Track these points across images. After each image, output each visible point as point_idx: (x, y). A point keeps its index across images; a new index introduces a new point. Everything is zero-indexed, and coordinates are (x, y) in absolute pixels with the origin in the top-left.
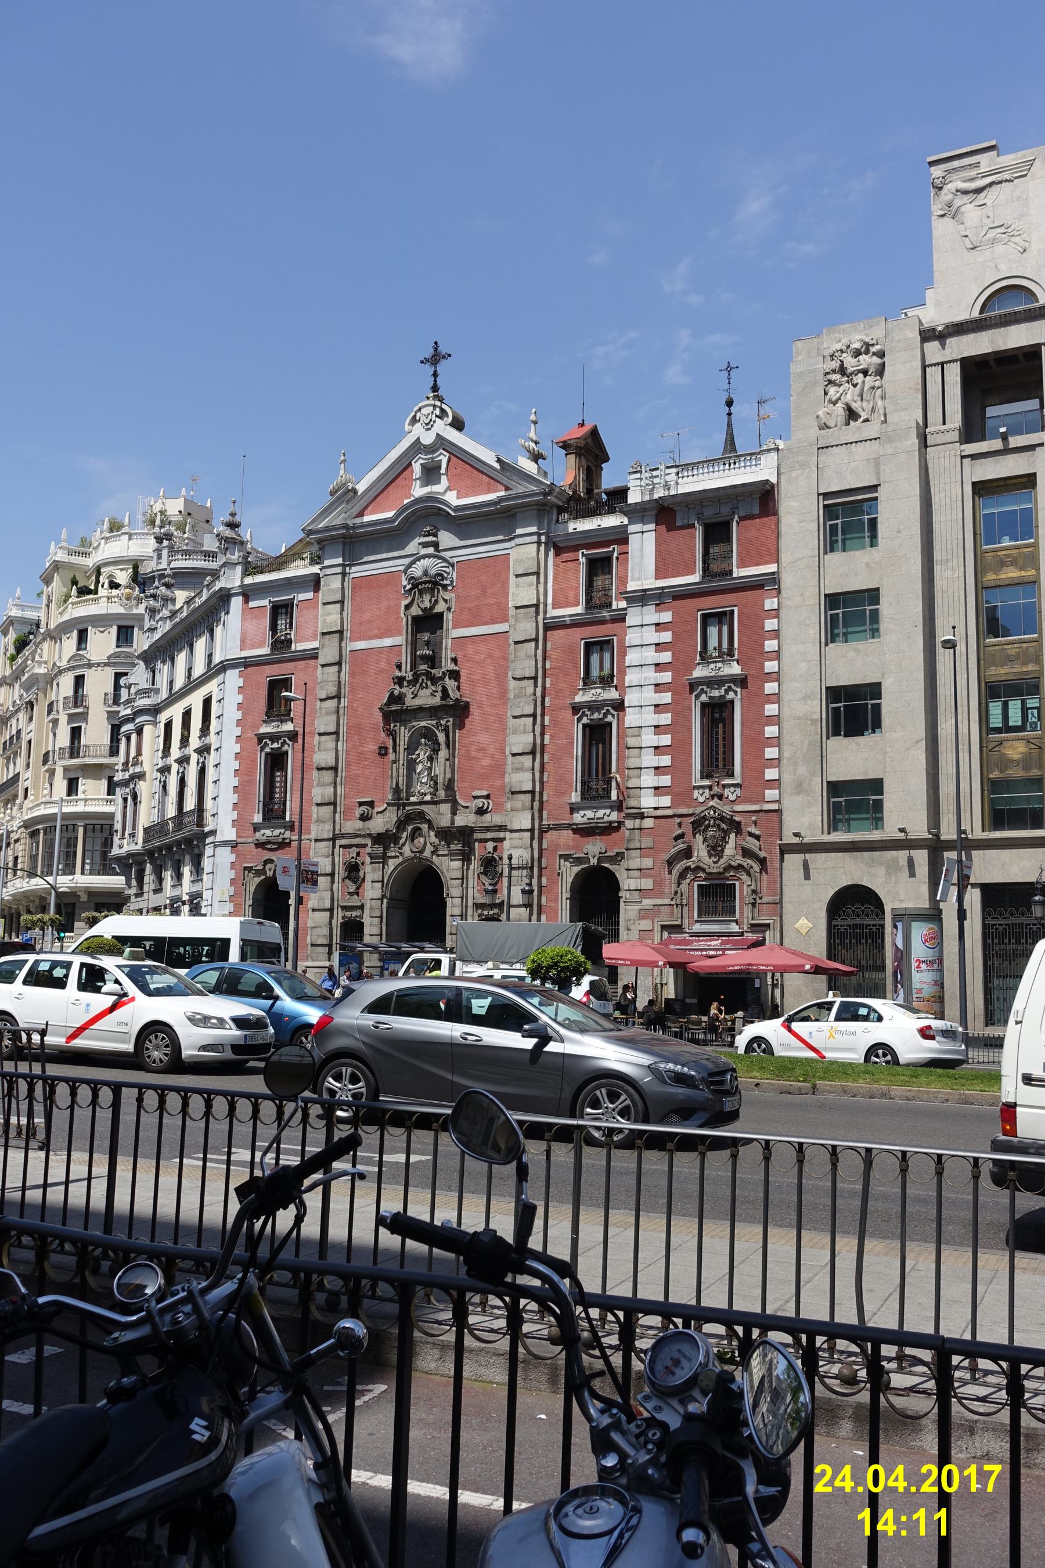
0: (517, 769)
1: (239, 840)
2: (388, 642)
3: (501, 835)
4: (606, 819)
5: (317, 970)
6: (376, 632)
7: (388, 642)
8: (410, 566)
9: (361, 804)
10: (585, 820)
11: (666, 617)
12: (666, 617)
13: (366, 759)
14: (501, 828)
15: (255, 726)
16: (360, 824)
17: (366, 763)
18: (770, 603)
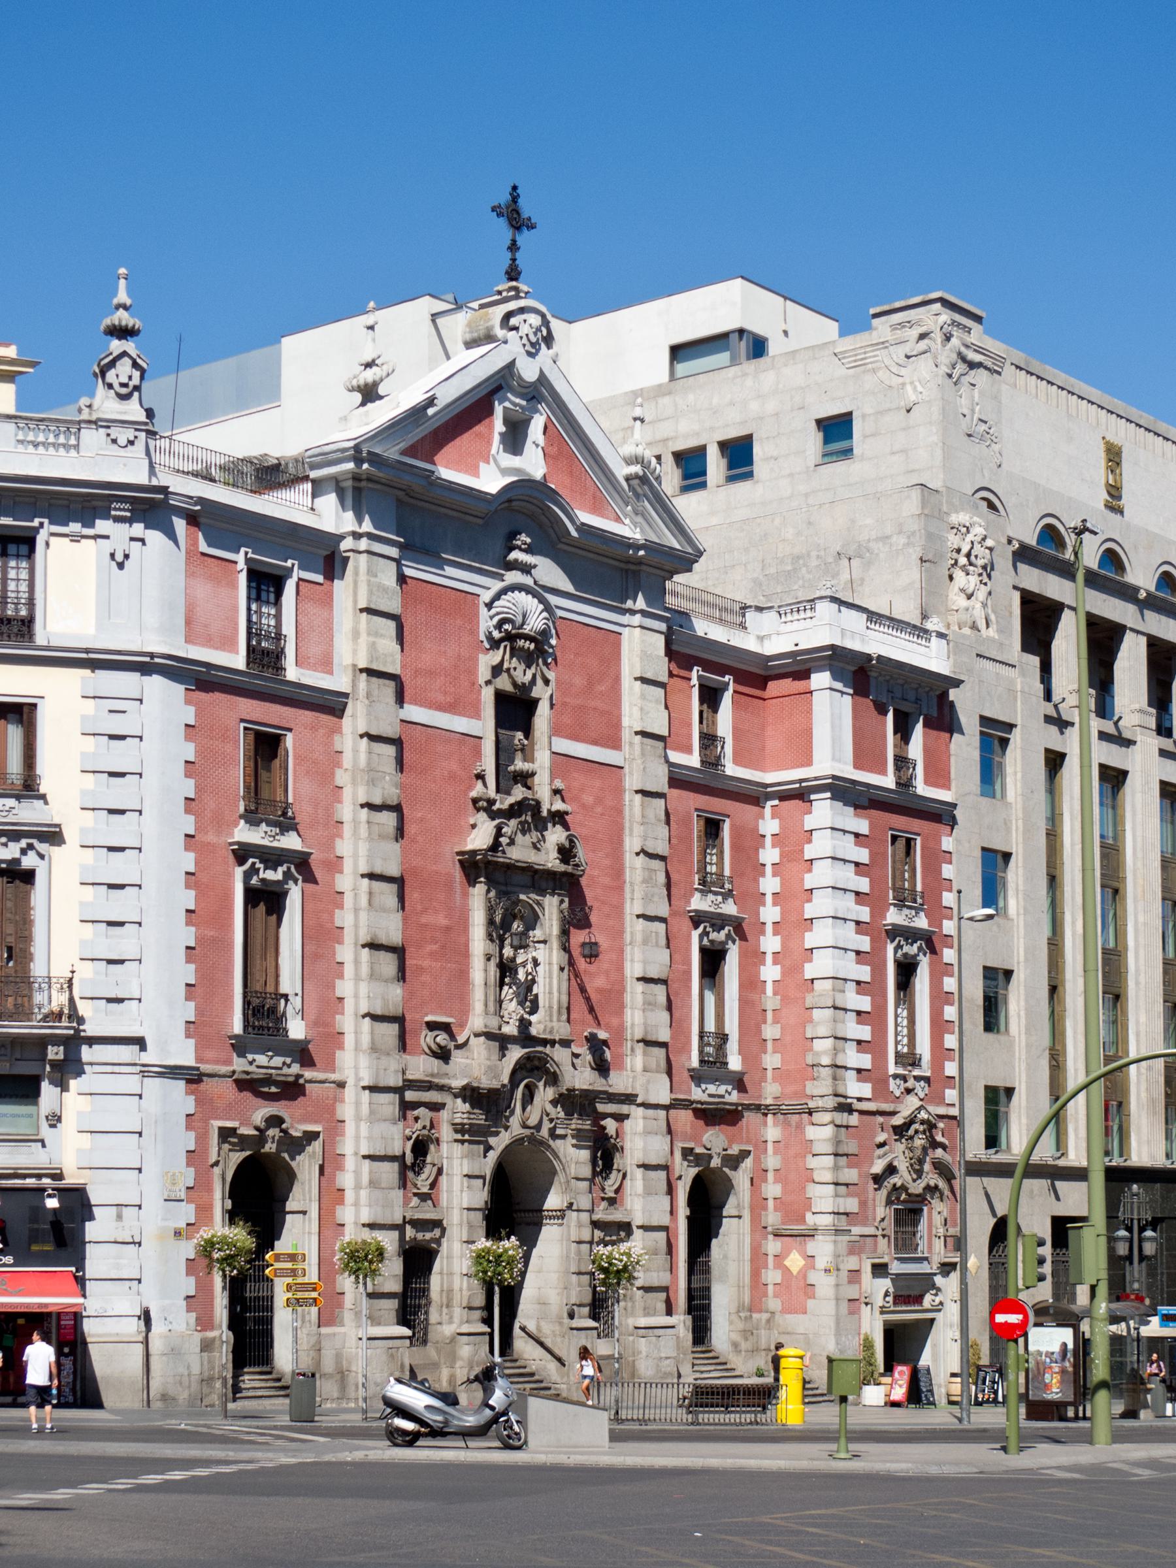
0: (650, 1004)
1: (206, 1068)
2: (460, 724)
3: (624, 1109)
4: (728, 1099)
5: (391, 1343)
6: (441, 698)
7: (460, 724)
8: (497, 597)
9: (432, 1026)
10: (705, 1098)
11: (863, 827)
12: (863, 827)
13: (434, 941)
14: (629, 1099)
15: (222, 824)
16: (435, 1064)
17: (435, 947)
18: (947, 843)
